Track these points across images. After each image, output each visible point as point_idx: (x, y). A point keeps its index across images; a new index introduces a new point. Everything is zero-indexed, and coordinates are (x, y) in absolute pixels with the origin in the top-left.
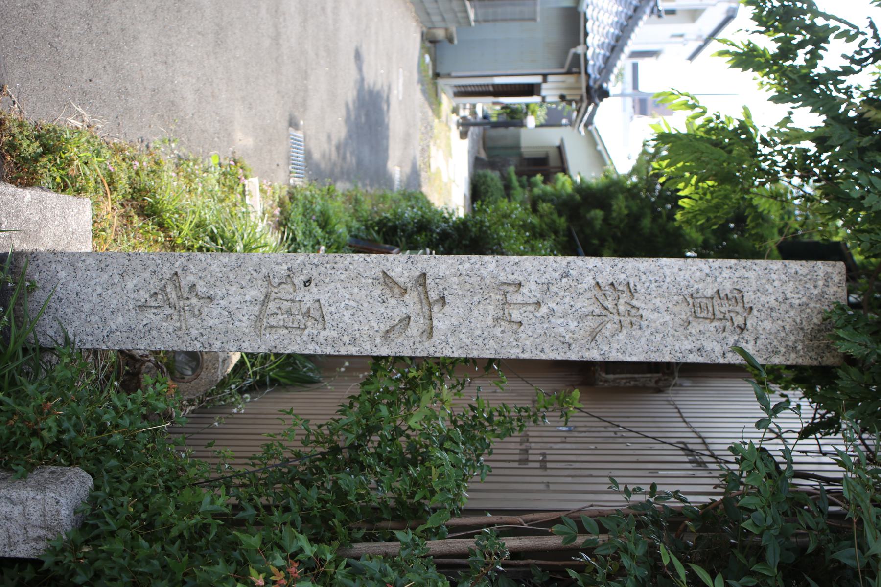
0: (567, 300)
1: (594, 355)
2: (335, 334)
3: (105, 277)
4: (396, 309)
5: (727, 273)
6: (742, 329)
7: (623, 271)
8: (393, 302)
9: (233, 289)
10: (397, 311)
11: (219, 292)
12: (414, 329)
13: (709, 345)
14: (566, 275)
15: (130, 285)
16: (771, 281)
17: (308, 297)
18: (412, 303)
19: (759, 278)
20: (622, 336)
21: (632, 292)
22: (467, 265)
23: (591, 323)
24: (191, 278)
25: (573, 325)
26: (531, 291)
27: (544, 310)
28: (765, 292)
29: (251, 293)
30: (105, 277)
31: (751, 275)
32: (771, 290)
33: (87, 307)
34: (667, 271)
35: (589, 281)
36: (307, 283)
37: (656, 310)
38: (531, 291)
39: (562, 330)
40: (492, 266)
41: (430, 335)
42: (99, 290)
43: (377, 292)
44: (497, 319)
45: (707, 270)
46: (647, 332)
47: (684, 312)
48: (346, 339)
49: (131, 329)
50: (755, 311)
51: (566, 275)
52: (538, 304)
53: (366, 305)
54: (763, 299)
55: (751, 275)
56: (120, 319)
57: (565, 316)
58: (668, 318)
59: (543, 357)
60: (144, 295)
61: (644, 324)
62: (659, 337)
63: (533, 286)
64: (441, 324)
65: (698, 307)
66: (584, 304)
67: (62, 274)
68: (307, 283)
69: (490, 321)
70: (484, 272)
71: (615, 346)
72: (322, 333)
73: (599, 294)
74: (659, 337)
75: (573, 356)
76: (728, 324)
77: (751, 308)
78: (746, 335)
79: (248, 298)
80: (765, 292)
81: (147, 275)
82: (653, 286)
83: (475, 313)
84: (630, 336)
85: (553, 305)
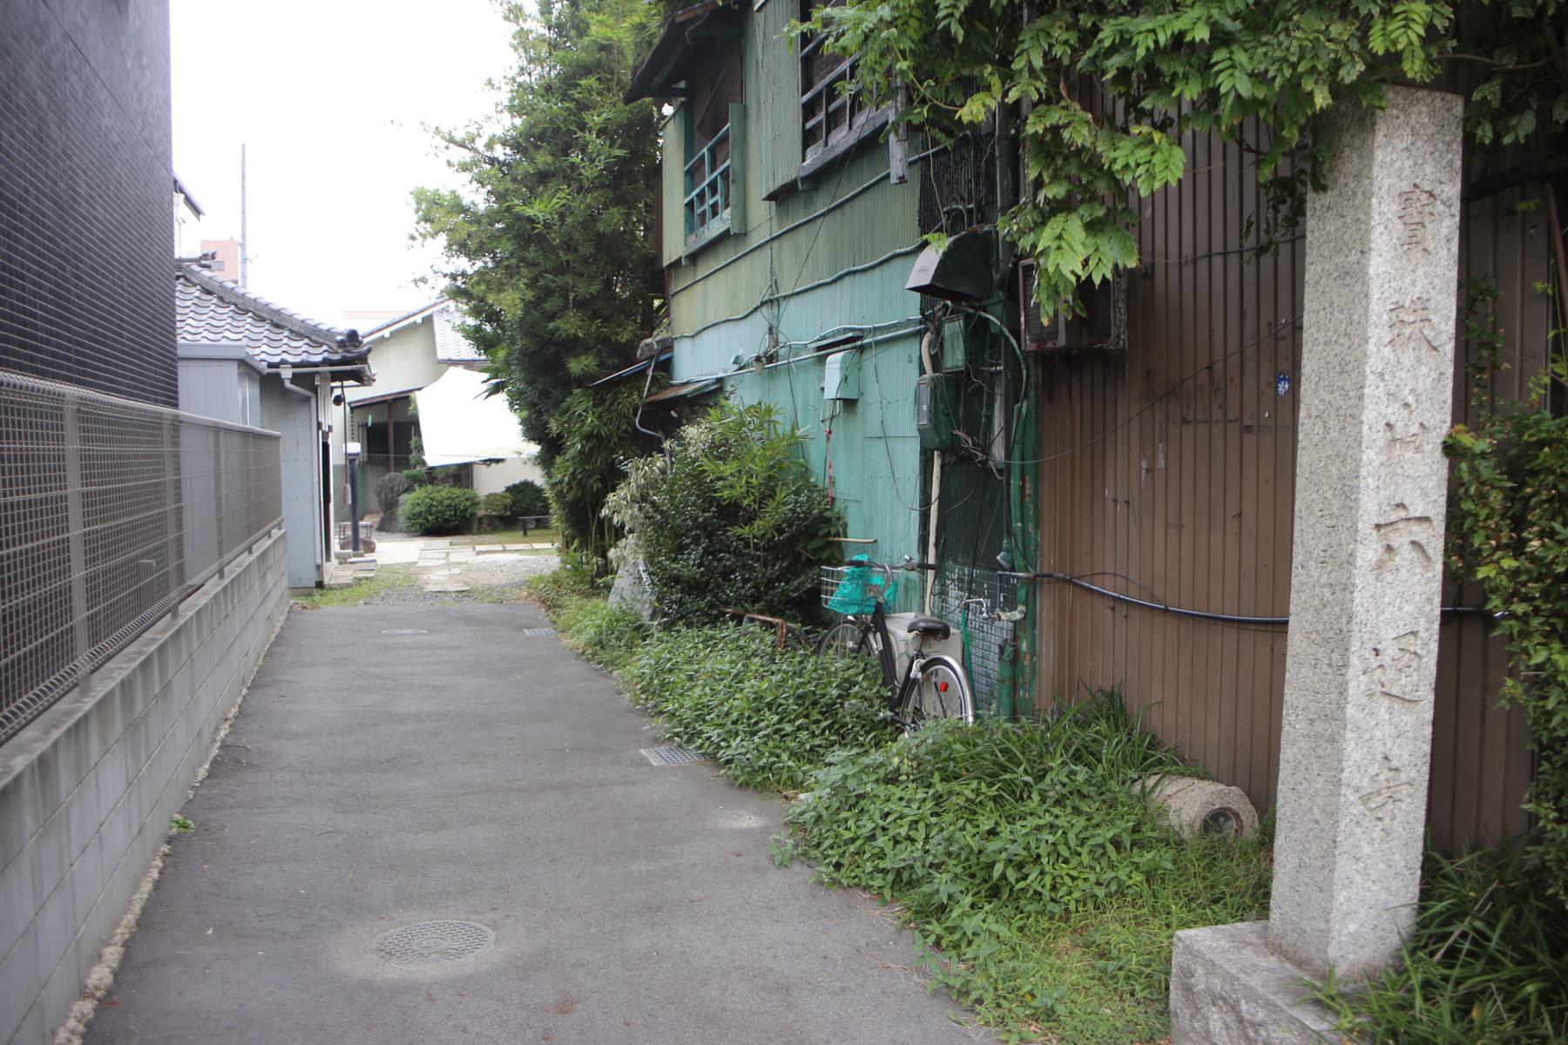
0: (1403, 375)
1: (1449, 348)
2: (1422, 620)
3: (1358, 879)
4: (1406, 554)
5: (1384, 208)
6: (1431, 194)
7: (1380, 316)
8: (1398, 559)
9: (1378, 734)
10: (1406, 555)
11: (1379, 749)
12: (1421, 538)
13: (1444, 232)
14: (1382, 374)
15: (1367, 849)
16: (1393, 162)
17: (1389, 650)
18: (1400, 540)
19: (1389, 175)
20: (1435, 320)
21: (1399, 307)
22: (1370, 480)
23: (1424, 352)
24: (1366, 781)
25: (1424, 370)
26: (1394, 413)
27: (1410, 400)
28: (1401, 170)
29: (1383, 713)
30: (1358, 879)
31: (1386, 183)
32: (1398, 164)
33: (1383, 896)
34: (1382, 269)
35: (1387, 352)
36: (1377, 652)
37: (1413, 283)
38: (1394, 413)
39: (1428, 381)
40: (1371, 453)
41: (1426, 519)
42: (1369, 884)
43: (1389, 577)
44: (1418, 449)
45: (1380, 229)
46: (1433, 293)
47: (1417, 253)
48: (1428, 608)
49: (1406, 845)
50: (1418, 181)
51: (1382, 374)
52: (1406, 405)
53: (1399, 588)
54: (1407, 172)
55: (1386, 183)
56: (1397, 857)
57: (1416, 378)
58: (1420, 272)
59: (1450, 401)
60: (1377, 833)
61: (1425, 296)
62: (1437, 281)
63: (1390, 410)
64: (1418, 510)
65: (1412, 240)
66: (1407, 359)
67: (1352, 927)
68: (1377, 652)
69: (1418, 456)
70: (1376, 464)
71: (1443, 327)
72: (1421, 634)
73: (1398, 341)
74: (1437, 281)
75: (1451, 370)
76: (1427, 209)
77: (1415, 186)
78: (1437, 192)
79: (1387, 717)
80: (1401, 170)
81: (1359, 831)
82: (1394, 285)
83: (1410, 472)
84: (1435, 312)
85: (1406, 391)
